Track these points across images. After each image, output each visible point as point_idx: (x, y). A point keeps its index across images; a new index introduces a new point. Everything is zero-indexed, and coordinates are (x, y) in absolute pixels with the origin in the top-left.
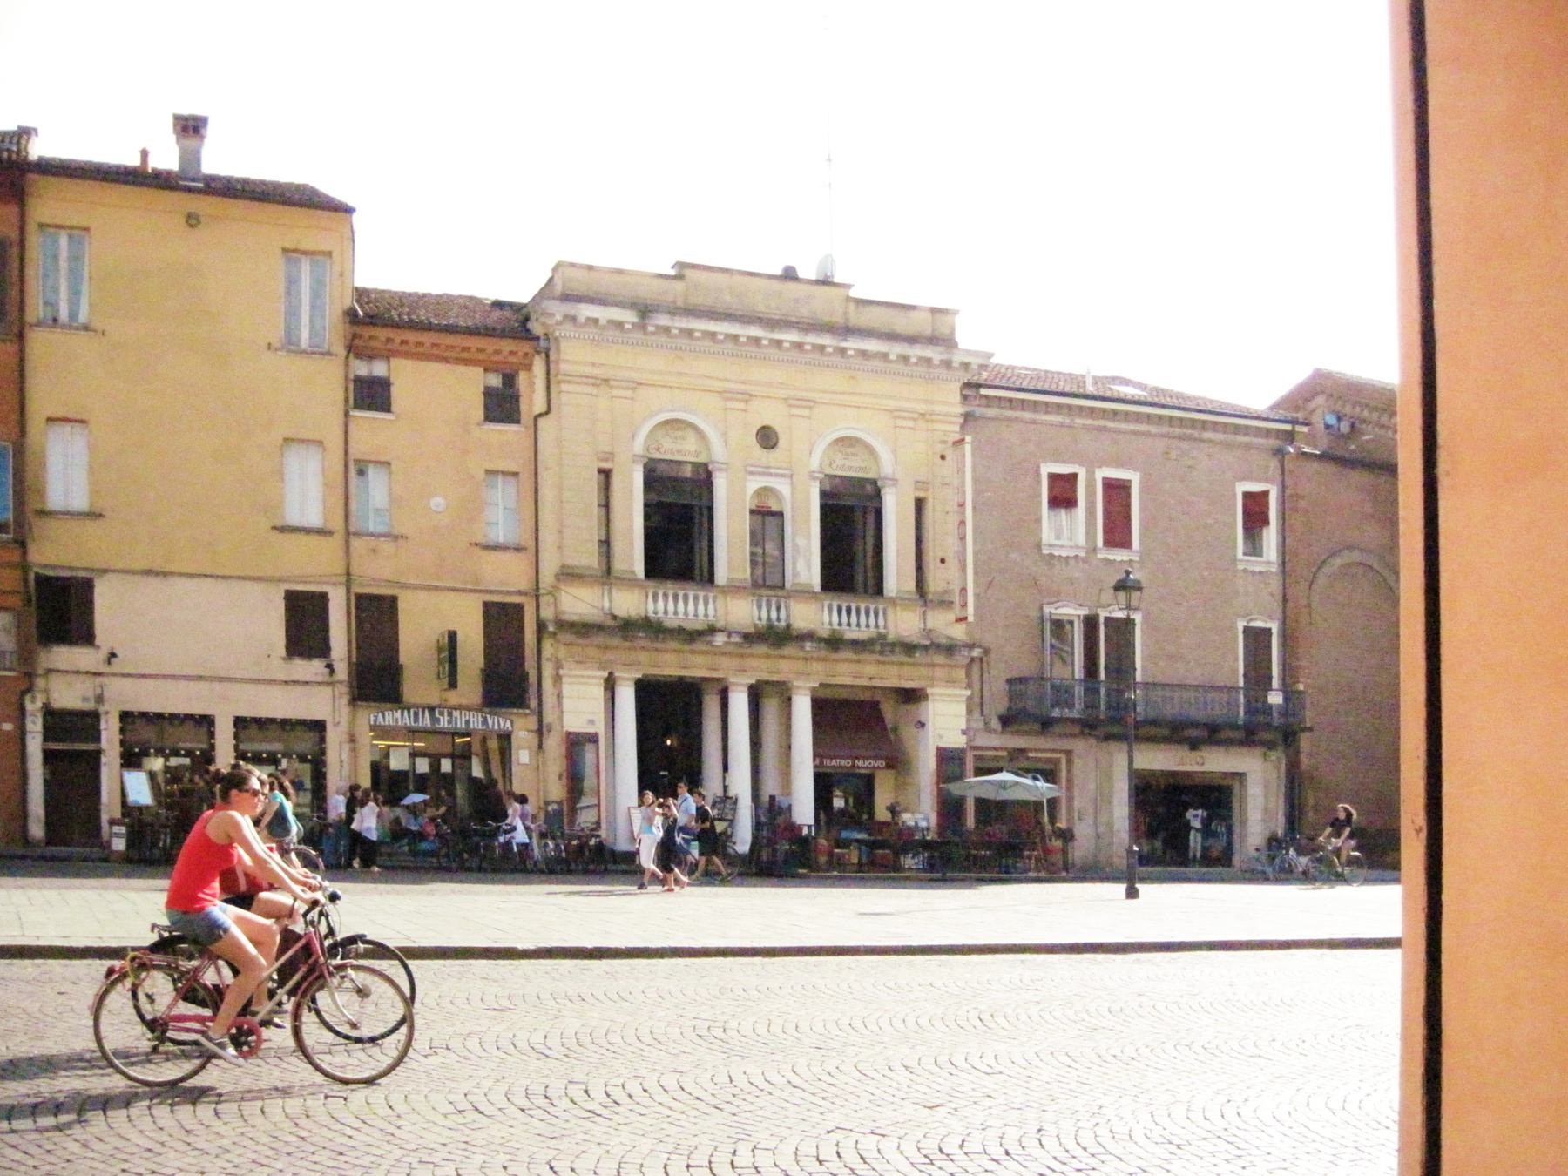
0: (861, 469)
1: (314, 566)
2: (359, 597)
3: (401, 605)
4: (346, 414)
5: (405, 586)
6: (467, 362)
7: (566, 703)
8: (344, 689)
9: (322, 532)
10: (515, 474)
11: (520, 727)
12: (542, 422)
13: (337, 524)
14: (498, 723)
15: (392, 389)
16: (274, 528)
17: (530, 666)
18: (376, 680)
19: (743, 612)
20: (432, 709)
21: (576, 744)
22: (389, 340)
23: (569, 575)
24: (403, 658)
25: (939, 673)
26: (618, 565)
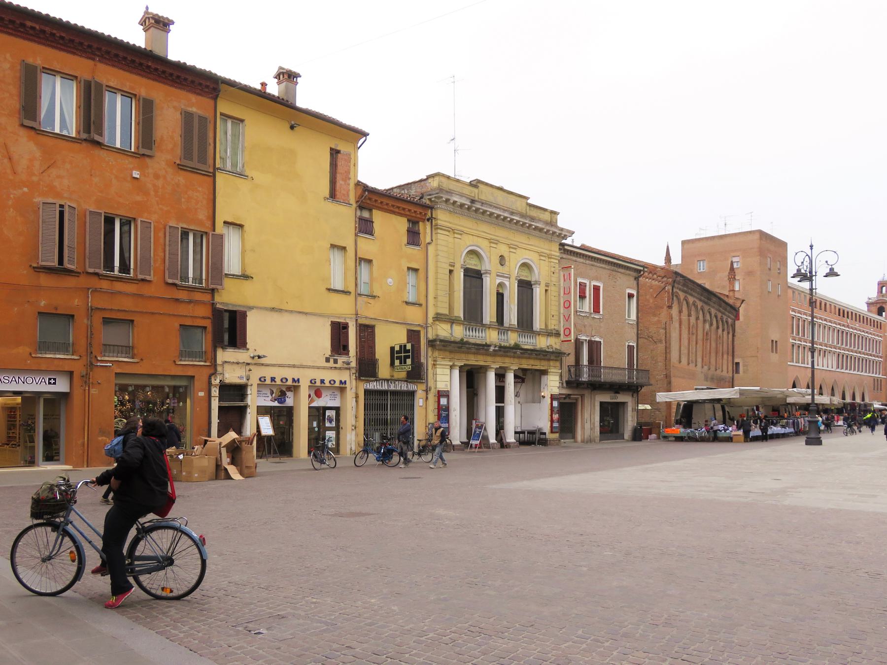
1: (343, 309)
3: (377, 330)
4: (356, 235)
7: (439, 378)
8: (354, 371)
9: (346, 292)
13: (352, 288)
14: (411, 387)
17: (423, 360)
18: (367, 368)
20: (388, 380)
21: (440, 394)
23: (438, 318)
24: (377, 357)
25: (552, 363)
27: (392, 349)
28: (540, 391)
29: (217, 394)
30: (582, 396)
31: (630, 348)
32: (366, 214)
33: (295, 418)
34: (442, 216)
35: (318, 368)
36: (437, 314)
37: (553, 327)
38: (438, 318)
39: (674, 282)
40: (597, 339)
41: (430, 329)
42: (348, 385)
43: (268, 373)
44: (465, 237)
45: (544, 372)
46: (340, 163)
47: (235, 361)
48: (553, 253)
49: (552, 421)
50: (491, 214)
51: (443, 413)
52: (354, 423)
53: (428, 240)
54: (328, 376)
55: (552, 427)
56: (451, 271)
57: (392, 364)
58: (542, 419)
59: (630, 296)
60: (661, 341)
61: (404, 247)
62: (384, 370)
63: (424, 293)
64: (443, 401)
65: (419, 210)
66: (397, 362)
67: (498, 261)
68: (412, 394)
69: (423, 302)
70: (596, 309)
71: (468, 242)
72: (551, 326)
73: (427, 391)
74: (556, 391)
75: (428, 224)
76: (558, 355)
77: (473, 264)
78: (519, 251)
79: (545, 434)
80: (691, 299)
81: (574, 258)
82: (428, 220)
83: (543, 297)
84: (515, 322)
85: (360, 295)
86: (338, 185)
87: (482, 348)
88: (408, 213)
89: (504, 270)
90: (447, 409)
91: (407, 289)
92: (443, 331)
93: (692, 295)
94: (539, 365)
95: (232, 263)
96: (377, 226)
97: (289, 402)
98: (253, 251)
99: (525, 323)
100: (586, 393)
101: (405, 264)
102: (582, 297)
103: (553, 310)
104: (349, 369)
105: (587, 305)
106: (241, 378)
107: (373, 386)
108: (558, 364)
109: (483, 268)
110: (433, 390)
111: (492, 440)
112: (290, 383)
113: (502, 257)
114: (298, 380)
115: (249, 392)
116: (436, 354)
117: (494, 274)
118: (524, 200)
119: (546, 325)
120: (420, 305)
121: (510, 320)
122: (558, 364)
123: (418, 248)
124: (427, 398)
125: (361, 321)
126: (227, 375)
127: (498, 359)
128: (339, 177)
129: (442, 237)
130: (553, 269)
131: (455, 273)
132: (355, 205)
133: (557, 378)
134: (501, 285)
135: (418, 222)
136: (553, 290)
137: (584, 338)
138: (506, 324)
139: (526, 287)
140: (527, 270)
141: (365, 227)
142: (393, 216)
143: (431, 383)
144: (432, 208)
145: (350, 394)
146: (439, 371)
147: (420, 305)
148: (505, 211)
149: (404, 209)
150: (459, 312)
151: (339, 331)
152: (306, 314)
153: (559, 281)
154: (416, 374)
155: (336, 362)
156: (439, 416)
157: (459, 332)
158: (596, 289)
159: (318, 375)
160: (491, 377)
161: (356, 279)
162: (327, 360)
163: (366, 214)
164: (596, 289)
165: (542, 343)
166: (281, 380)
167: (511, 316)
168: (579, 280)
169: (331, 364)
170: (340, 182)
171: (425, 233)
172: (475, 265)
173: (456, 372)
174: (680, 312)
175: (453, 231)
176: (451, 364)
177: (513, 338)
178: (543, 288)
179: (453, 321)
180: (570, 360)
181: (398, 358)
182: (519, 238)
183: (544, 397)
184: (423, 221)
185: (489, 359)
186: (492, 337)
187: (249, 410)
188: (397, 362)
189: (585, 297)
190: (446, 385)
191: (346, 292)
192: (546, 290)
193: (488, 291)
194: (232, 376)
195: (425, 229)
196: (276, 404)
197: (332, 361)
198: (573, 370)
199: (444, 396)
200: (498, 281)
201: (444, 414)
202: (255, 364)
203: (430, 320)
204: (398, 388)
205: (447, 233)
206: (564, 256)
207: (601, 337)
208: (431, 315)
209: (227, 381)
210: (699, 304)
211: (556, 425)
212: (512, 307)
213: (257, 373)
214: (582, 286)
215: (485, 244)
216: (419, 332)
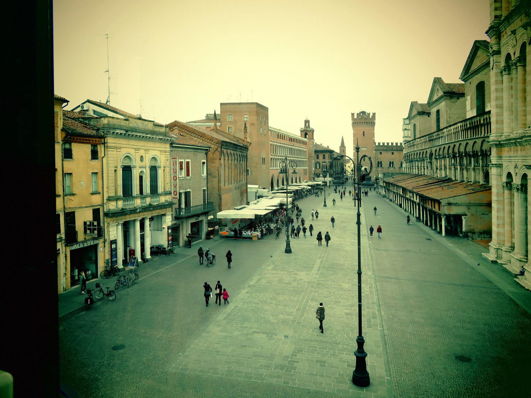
0: (128, 163)
4: (63, 160)
10: (97, 173)
11: (100, 242)
14: (96, 242)
15: (73, 152)
20: (83, 242)
22: (77, 139)
23: (109, 199)
24: (77, 229)
25: (168, 209)
27: (85, 223)
28: (162, 225)
30: (182, 223)
31: (204, 190)
32: (67, 146)
34: (110, 141)
36: (109, 197)
37: (168, 190)
38: (109, 199)
39: (222, 146)
40: (189, 190)
41: (105, 206)
44: (122, 150)
45: (164, 215)
48: (167, 149)
49: (168, 241)
50: (136, 136)
51: (113, 253)
53: (103, 155)
55: (168, 244)
56: (115, 170)
57: (85, 232)
58: (163, 240)
59: (204, 163)
60: (216, 177)
61: (89, 161)
62: (81, 237)
63: (101, 186)
64: (114, 246)
65: (97, 140)
66: (88, 232)
67: (139, 159)
69: (100, 190)
70: (188, 175)
71: (124, 152)
72: (167, 190)
73: (104, 242)
75: (103, 146)
76: (170, 205)
77: (127, 163)
78: (150, 151)
79: (165, 248)
80: (229, 151)
81: (177, 149)
82: (102, 144)
83: (162, 174)
85: (66, 195)
87: (134, 211)
88: (91, 142)
89: (143, 164)
90: (116, 249)
92: (112, 206)
93: (229, 149)
94: (161, 212)
96: (74, 153)
100: (184, 221)
102: (181, 169)
103: (168, 180)
105: (184, 172)
107: (75, 247)
108: (170, 209)
109: (132, 165)
111: (140, 260)
116: (109, 220)
117: (138, 168)
118: (152, 123)
119: (164, 189)
120: (99, 193)
122: (170, 209)
123: (97, 160)
124: (105, 246)
125: (66, 212)
127: (141, 214)
132: (61, 142)
133: (170, 217)
134: (142, 172)
135: (97, 145)
136: (167, 169)
137: (182, 191)
138: (144, 194)
139: (154, 169)
140: (154, 160)
142: (83, 145)
143: (106, 237)
144: (104, 137)
146: (111, 229)
148: (143, 133)
149: (89, 140)
150: (120, 193)
153: (170, 165)
154: (101, 234)
156: (111, 255)
157: (120, 204)
158: (188, 163)
160: (138, 224)
161: (63, 186)
163: (67, 146)
164: (188, 163)
165: (163, 199)
167: (147, 189)
173: (120, 227)
174: (224, 160)
175: (116, 148)
177: (148, 201)
178: (162, 169)
179: (117, 199)
180: (177, 206)
181: (89, 229)
182: (150, 145)
184: (100, 144)
185: (136, 215)
186: (138, 203)
188: (88, 232)
195: (100, 149)
198: (178, 210)
199: (113, 243)
200: (140, 171)
201: (114, 253)
203: (105, 201)
204: (89, 245)
206: (172, 149)
207: (190, 188)
208: (105, 198)
210: (232, 152)
211: (170, 242)
214: (181, 163)
215: (132, 151)
216: (99, 209)
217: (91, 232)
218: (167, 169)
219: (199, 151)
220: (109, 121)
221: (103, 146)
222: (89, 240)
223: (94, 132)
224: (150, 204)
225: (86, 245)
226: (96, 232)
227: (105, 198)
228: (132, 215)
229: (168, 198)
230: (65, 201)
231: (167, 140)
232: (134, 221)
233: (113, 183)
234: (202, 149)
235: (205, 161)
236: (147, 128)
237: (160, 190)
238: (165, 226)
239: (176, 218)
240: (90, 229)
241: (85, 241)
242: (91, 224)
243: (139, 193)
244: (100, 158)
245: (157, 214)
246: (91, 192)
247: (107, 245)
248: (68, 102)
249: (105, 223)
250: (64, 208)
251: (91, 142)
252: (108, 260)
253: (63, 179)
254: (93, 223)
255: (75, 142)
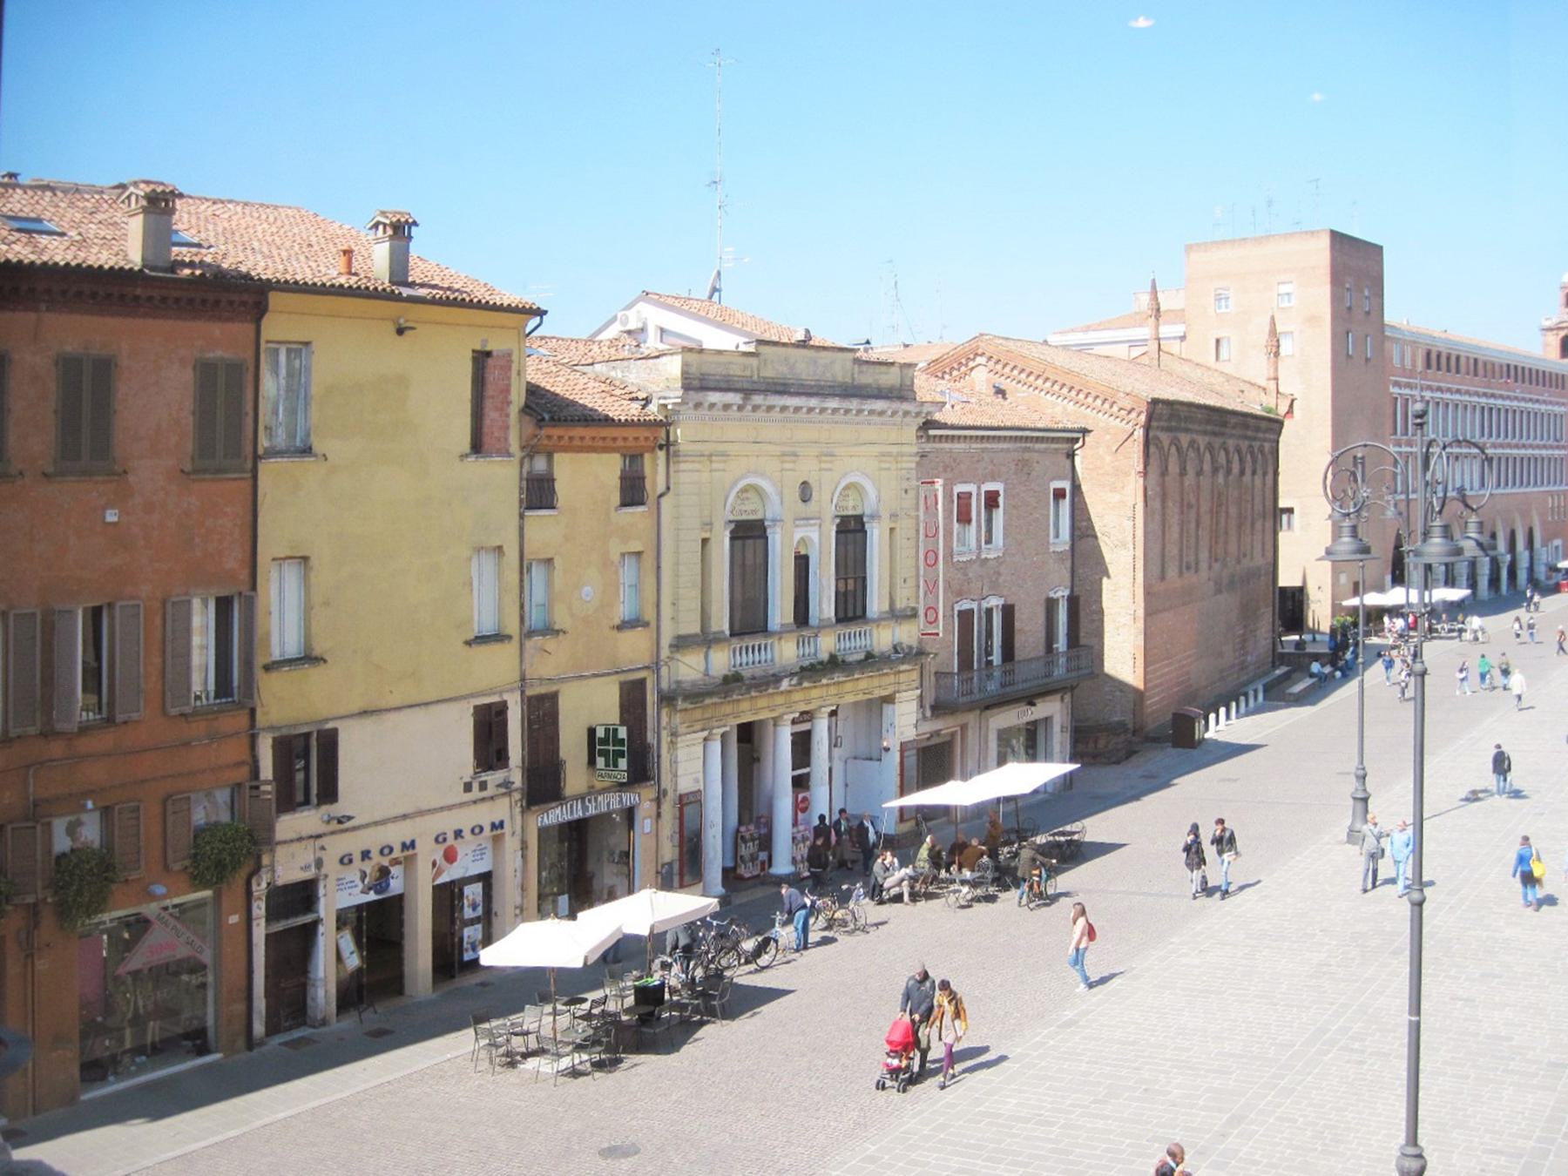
1: (494, 674)
2: (530, 698)
4: (522, 516)
5: (562, 680)
6: (605, 450)
8: (517, 796)
9: (499, 637)
10: (639, 554)
11: (643, 799)
12: (664, 500)
13: (512, 627)
14: (629, 798)
15: (557, 486)
16: (468, 643)
17: (651, 737)
18: (543, 784)
19: (787, 652)
23: (682, 643)
24: (563, 754)
25: (903, 677)
26: (714, 628)
27: (592, 732)
29: (263, 912)
33: (406, 917)
35: (450, 808)
36: (679, 638)
38: (682, 643)
41: (664, 671)
42: (507, 829)
43: (352, 843)
45: (889, 700)
46: (493, 375)
47: (294, 836)
48: (905, 449)
52: (518, 900)
53: (661, 488)
54: (466, 819)
56: (705, 541)
57: (592, 762)
59: (1059, 494)
61: (613, 514)
62: (575, 778)
63: (652, 598)
68: (630, 814)
69: (650, 615)
74: (910, 734)
75: (661, 454)
82: (661, 447)
84: (829, 611)
86: (487, 422)
91: (616, 596)
92: (689, 668)
95: (282, 630)
97: (396, 886)
98: (326, 604)
99: (851, 609)
101: (615, 548)
103: (905, 566)
104: (509, 794)
106: (306, 868)
107: (556, 815)
109: (769, 515)
110: (670, 794)
112: (397, 853)
113: (805, 485)
114: (413, 844)
115: (321, 891)
118: (850, 356)
120: (646, 625)
121: (821, 610)
123: (640, 509)
124: (659, 815)
125: (530, 692)
126: (279, 869)
127: (797, 696)
128: (488, 404)
129: (688, 476)
130: (905, 485)
131: (713, 545)
133: (914, 706)
135: (642, 455)
139: (852, 530)
141: (539, 493)
142: (594, 456)
143: (666, 782)
145: (511, 844)
146: (682, 754)
147: (646, 625)
149: (615, 439)
150: (721, 621)
151: (489, 725)
152: (426, 704)
154: (642, 769)
155: (483, 786)
157: (721, 661)
159: (447, 823)
161: (522, 607)
162: (468, 788)
163: (540, 464)
165: (883, 638)
166: (381, 852)
167: (824, 604)
168: (959, 488)
169: (476, 793)
170: (491, 415)
171: (655, 472)
172: (754, 512)
173: (716, 747)
176: (705, 734)
177: (827, 644)
178: (887, 524)
179: (705, 640)
181: (602, 753)
183: (887, 750)
184: (652, 450)
187: (321, 929)
188: (600, 762)
189: (969, 521)
190: (697, 781)
191: (499, 637)
192: (892, 530)
193: (778, 561)
194: (288, 867)
195: (655, 470)
196: (372, 896)
197: (476, 786)
202: (333, 833)
205: (697, 466)
206: (928, 447)
208: (666, 641)
209: (280, 882)
212: (825, 582)
213: (337, 846)
214: (964, 499)
216: (642, 682)
217: (607, 765)
218: (905, 527)
219: (1038, 446)
220: (685, 365)
221: (661, 454)
222: (604, 791)
223: (634, 410)
224: (833, 658)
225: (592, 811)
226: (623, 763)
227: (666, 641)
228: (762, 703)
229: (907, 634)
230: (526, 655)
231: (906, 413)
232: (776, 721)
233: (695, 588)
234: (1053, 440)
235: (1066, 485)
236: (828, 376)
237: (876, 603)
238: (892, 741)
239: (939, 709)
240: (604, 753)
241: (592, 792)
242: (611, 733)
243: (790, 618)
244: (651, 500)
245: (861, 697)
246: (617, 621)
247: (668, 809)
248: (541, 313)
249: (664, 734)
250: (523, 679)
251: (620, 443)
252: (670, 864)
253: (521, 581)
254: (615, 731)
255: (566, 449)
